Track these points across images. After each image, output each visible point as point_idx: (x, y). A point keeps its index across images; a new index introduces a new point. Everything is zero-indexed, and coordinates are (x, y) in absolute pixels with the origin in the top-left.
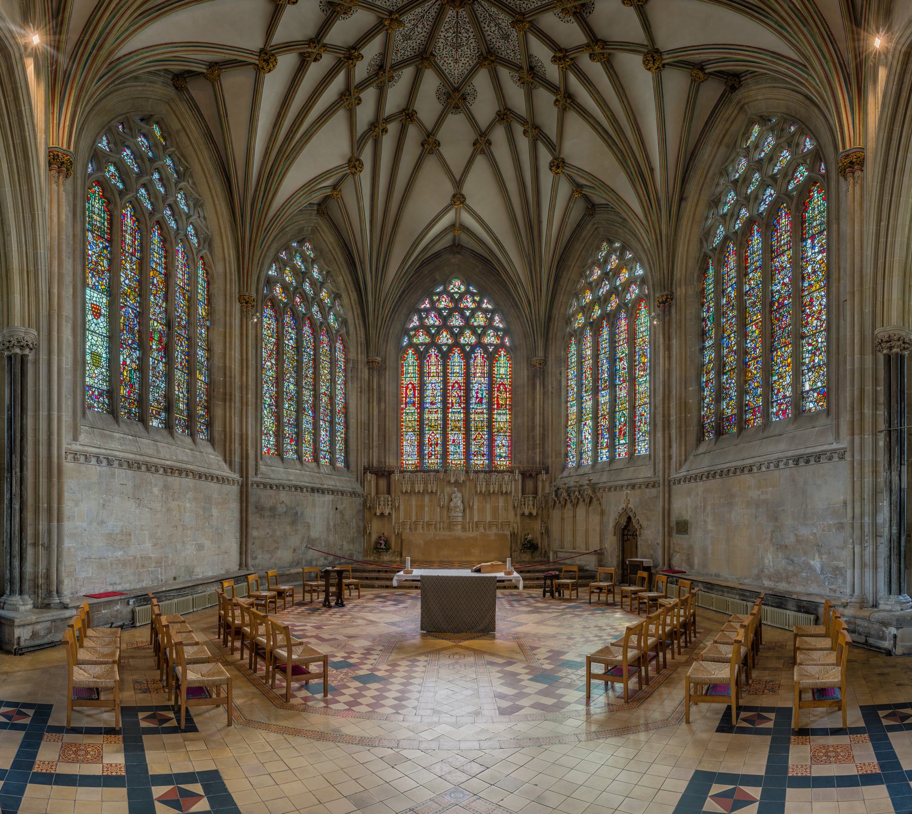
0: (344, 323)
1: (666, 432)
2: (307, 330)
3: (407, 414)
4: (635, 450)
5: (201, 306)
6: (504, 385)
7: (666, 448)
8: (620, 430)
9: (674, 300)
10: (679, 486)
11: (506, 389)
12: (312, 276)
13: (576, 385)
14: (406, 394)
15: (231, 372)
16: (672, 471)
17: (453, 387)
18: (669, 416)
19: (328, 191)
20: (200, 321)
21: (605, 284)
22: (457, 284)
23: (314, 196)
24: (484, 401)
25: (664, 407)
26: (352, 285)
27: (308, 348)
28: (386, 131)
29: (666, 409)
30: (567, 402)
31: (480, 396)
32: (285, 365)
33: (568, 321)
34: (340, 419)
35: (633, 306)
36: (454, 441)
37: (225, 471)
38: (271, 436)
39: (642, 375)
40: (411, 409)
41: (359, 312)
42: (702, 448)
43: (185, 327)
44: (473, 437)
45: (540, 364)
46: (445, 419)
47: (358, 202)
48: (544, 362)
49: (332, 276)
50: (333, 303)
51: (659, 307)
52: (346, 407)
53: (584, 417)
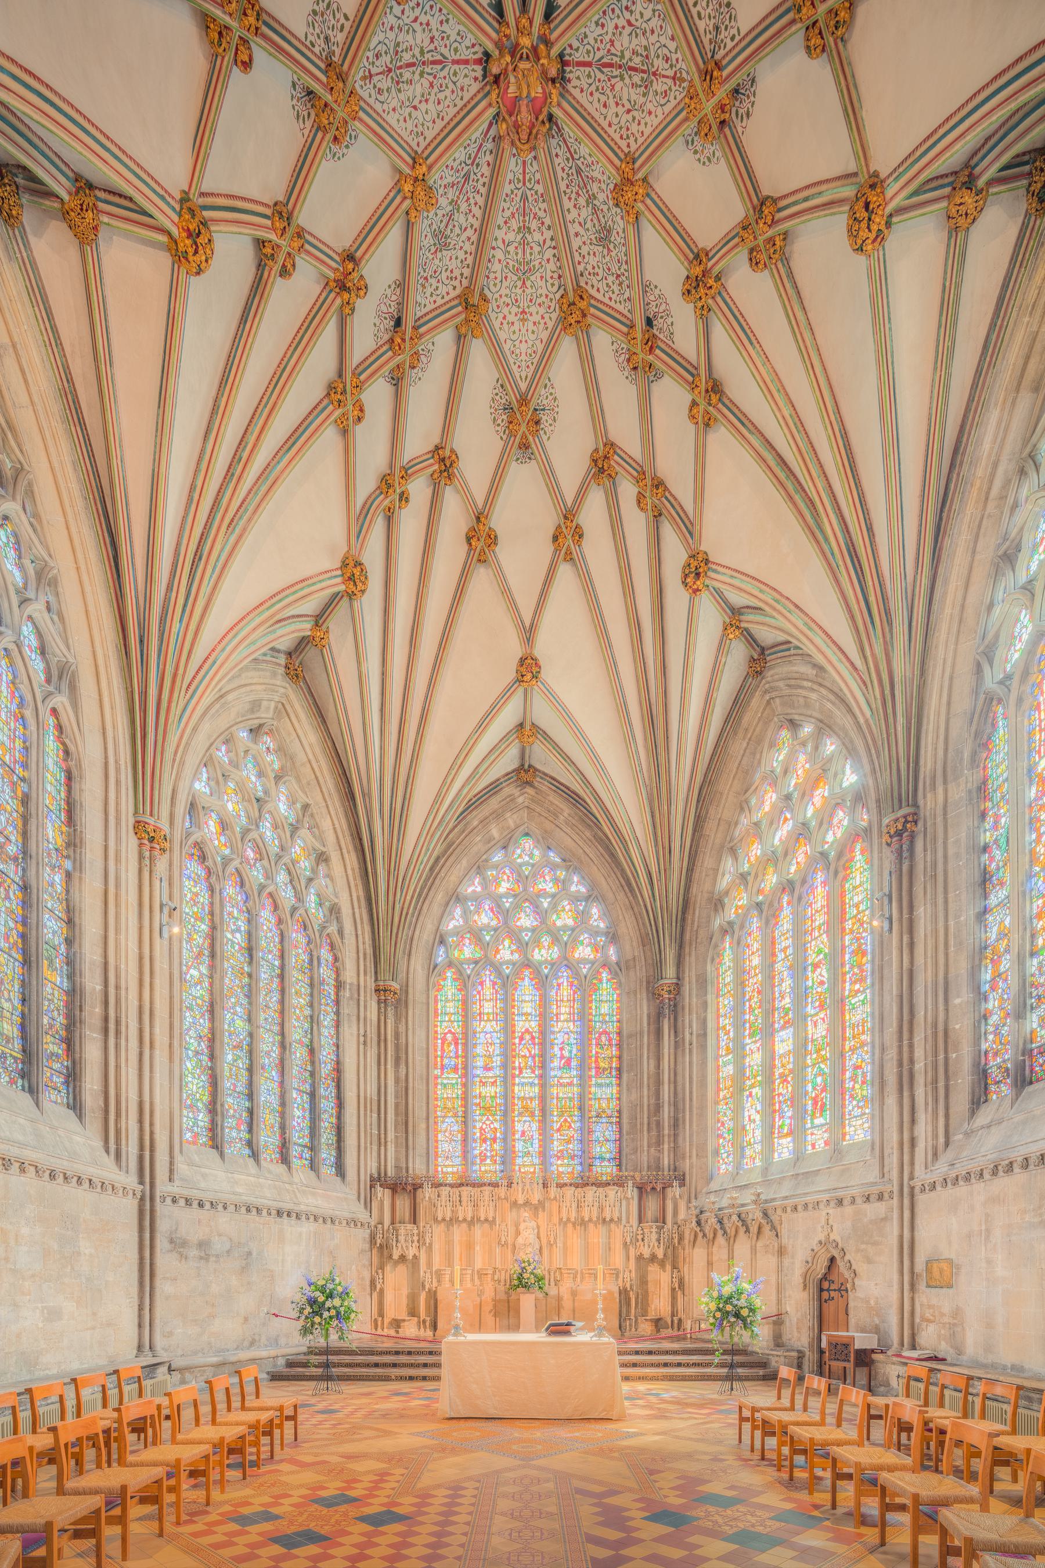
0: (334, 911)
1: (906, 1094)
2: (266, 916)
3: (445, 1086)
4: (844, 1135)
5: (53, 823)
6: (605, 1032)
7: (906, 1125)
8: (815, 1103)
9: (920, 824)
10: (933, 1194)
11: (610, 1040)
12: (277, 808)
13: (733, 1025)
14: (443, 1050)
15: (118, 977)
16: (917, 1167)
17: (521, 1039)
18: (912, 1061)
19: (305, 627)
20: (49, 855)
21: (786, 819)
22: (527, 846)
23: (280, 632)
24: (574, 1063)
25: (900, 1047)
26: (349, 839)
27: (270, 952)
28: (407, 500)
29: (905, 1049)
30: (717, 1057)
31: (566, 1054)
32: (227, 981)
33: (718, 904)
34: (326, 1091)
35: (840, 855)
36: (523, 1133)
37: (106, 1169)
38: (199, 1111)
39: (858, 991)
40: (453, 1078)
41: (361, 893)
42: (984, 1116)
43: (15, 859)
44: (556, 1126)
45: (670, 992)
46: (507, 1096)
47: (359, 662)
48: (678, 986)
49: (312, 815)
50: (314, 871)
51: (888, 845)
52: (338, 1069)
53: (748, 1083)
